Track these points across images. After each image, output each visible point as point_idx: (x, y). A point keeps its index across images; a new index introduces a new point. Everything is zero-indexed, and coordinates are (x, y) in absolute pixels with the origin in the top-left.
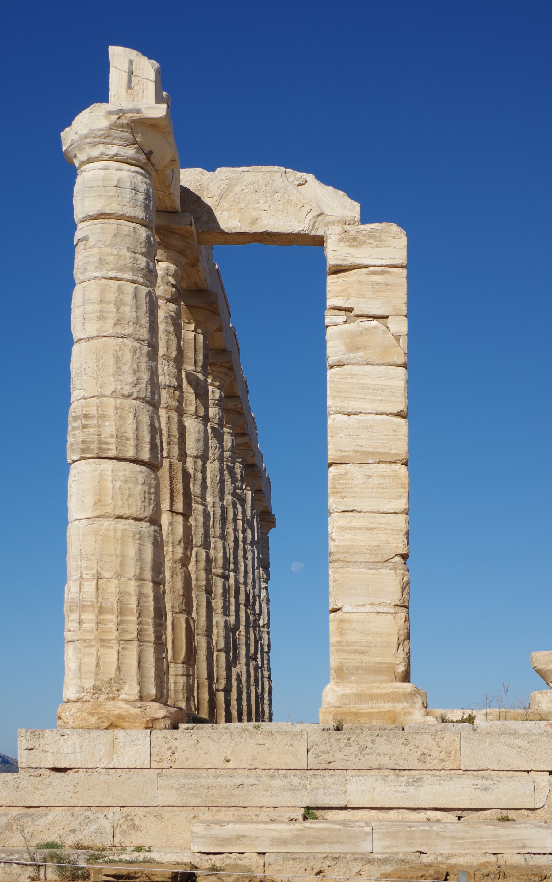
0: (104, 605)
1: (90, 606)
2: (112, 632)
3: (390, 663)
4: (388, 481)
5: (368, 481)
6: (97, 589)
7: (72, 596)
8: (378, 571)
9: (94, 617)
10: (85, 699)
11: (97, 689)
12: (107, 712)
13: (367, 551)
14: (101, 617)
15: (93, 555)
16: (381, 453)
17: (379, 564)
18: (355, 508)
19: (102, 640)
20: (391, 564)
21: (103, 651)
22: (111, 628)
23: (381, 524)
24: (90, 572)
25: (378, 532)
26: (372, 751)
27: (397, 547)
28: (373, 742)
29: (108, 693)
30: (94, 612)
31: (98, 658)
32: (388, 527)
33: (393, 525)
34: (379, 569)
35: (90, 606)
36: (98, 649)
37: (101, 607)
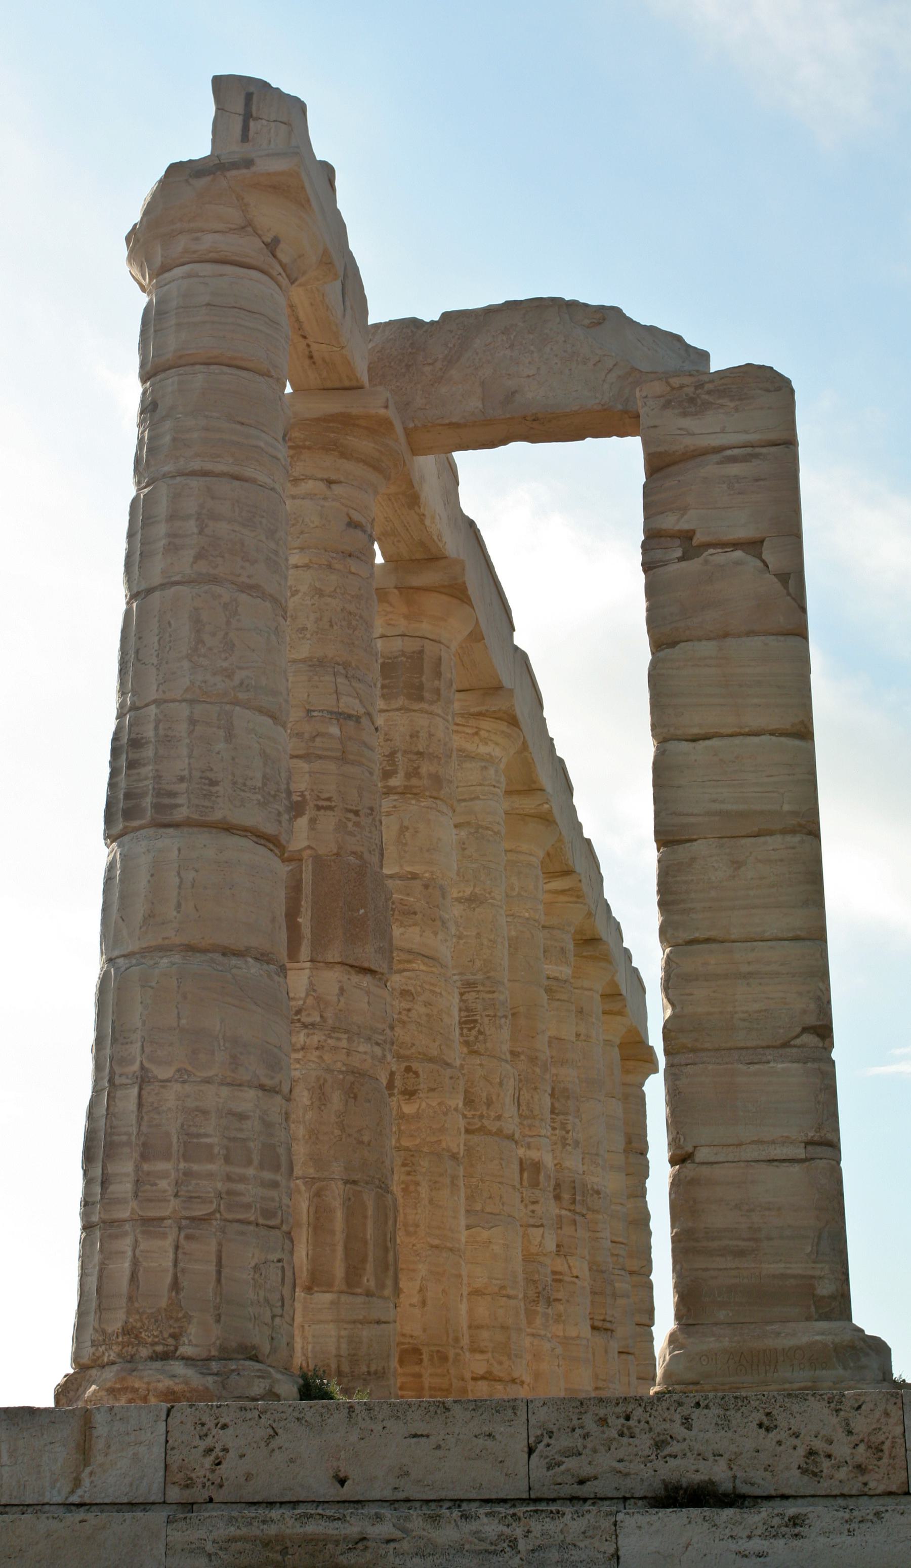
3: (803, 1277)
6: (140, 1105)
8: (766, 1066)
12: (145, 1386)
17: (768, 1051)
19: (146, 1221)
22: (165, 1191)
26: (684, 1446)
28: (687, 1422)
29: (153, 1344)
31: (135, 1263)
34: (768, 1062)
36: (136, 1241)
37: (144, 1145)
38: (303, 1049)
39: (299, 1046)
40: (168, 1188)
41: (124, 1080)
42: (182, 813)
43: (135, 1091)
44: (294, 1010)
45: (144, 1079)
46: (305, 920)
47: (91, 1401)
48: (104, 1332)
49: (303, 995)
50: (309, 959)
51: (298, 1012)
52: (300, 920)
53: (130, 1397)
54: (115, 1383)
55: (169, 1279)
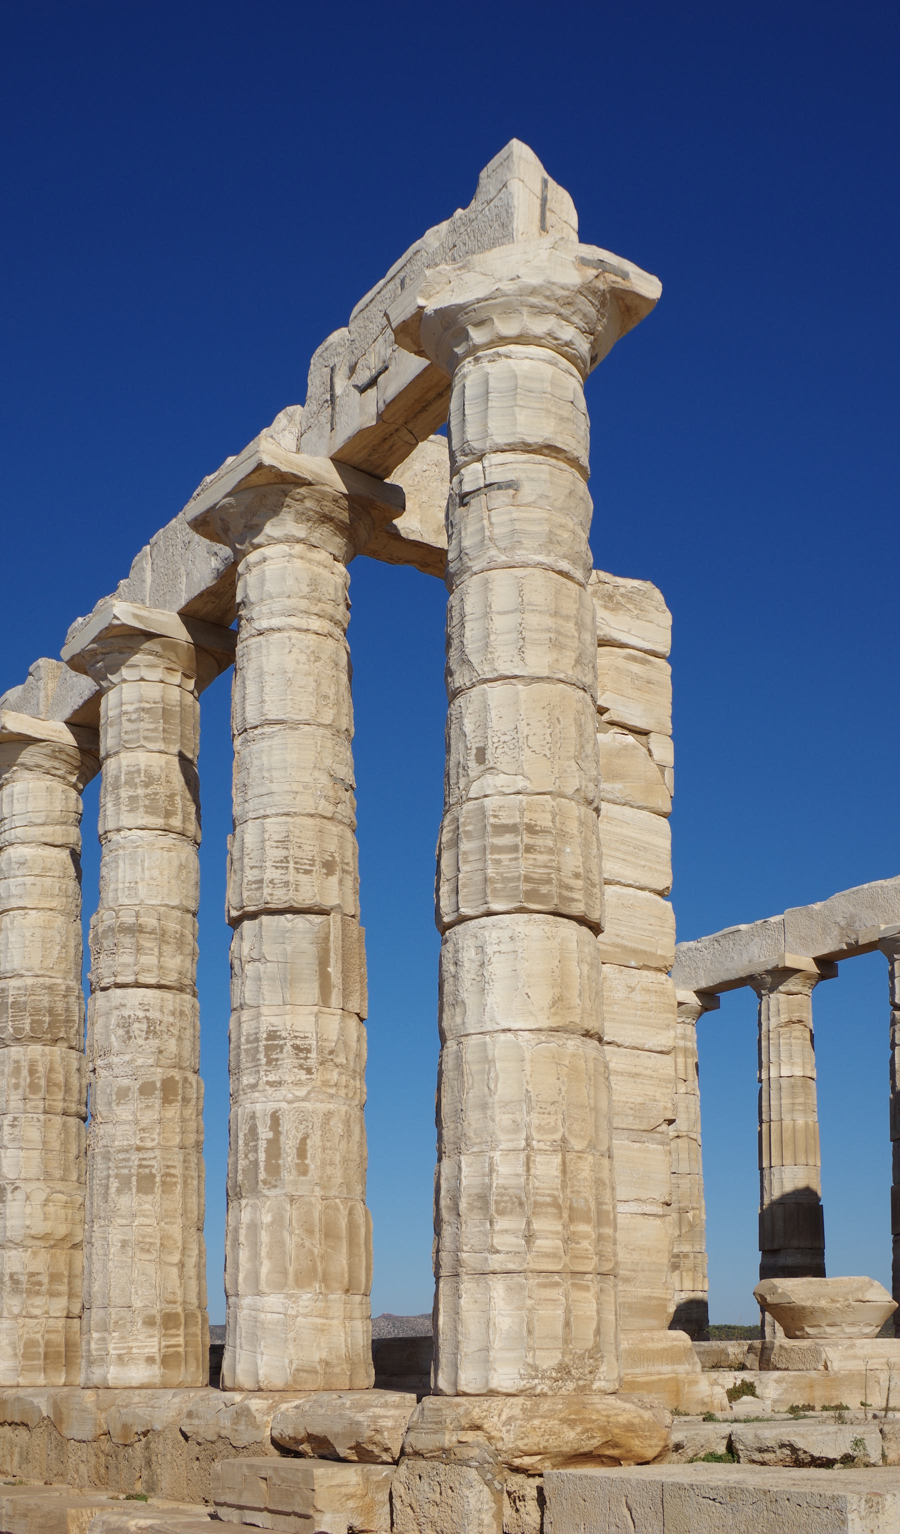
0: (575, 1205)
1: (549, 1205)
2: (587, 1258)
3: (661, 1299)
4: (654, 998)
5: (631, 996)
6: (564, 1171)
7: (501, 1181)
9: (560, 1228)
10: (538, 1391)
11: (564, 1370)
13: (631, 1112)
14: (572, 1228)
15: (552, 1103)
16: (645, 952)
18: (616, 1039)
20: (659, 1135)
21: (575, 1294)
22: (587, 1250)
23: (646, 1068)
24: (545, 1137)
25: (644, 1081)
27: (666, 1108)
29: (580, 1379)
30: (561, 1217)
31: (568, 1311)
32: (654, 1074)
33: (661, 1071)
35: (549, 1205)
38: (336, 1085)
39: (332, 1083)
40: (589, 1247)
41: (542, 1145)
42: (577, 909)
43: (557, 1159)
44: (328, 1050)
45: (563, 1146)
46: (334, 970)
47: (540, 1428)
48: (536, 1369)
49: (335, 1038)
50: (341, 1006)
51: (331, 1053)
52: (330, 970)
53: (588, 1426)
54: (571, 1414)
55: (594, 1326)
